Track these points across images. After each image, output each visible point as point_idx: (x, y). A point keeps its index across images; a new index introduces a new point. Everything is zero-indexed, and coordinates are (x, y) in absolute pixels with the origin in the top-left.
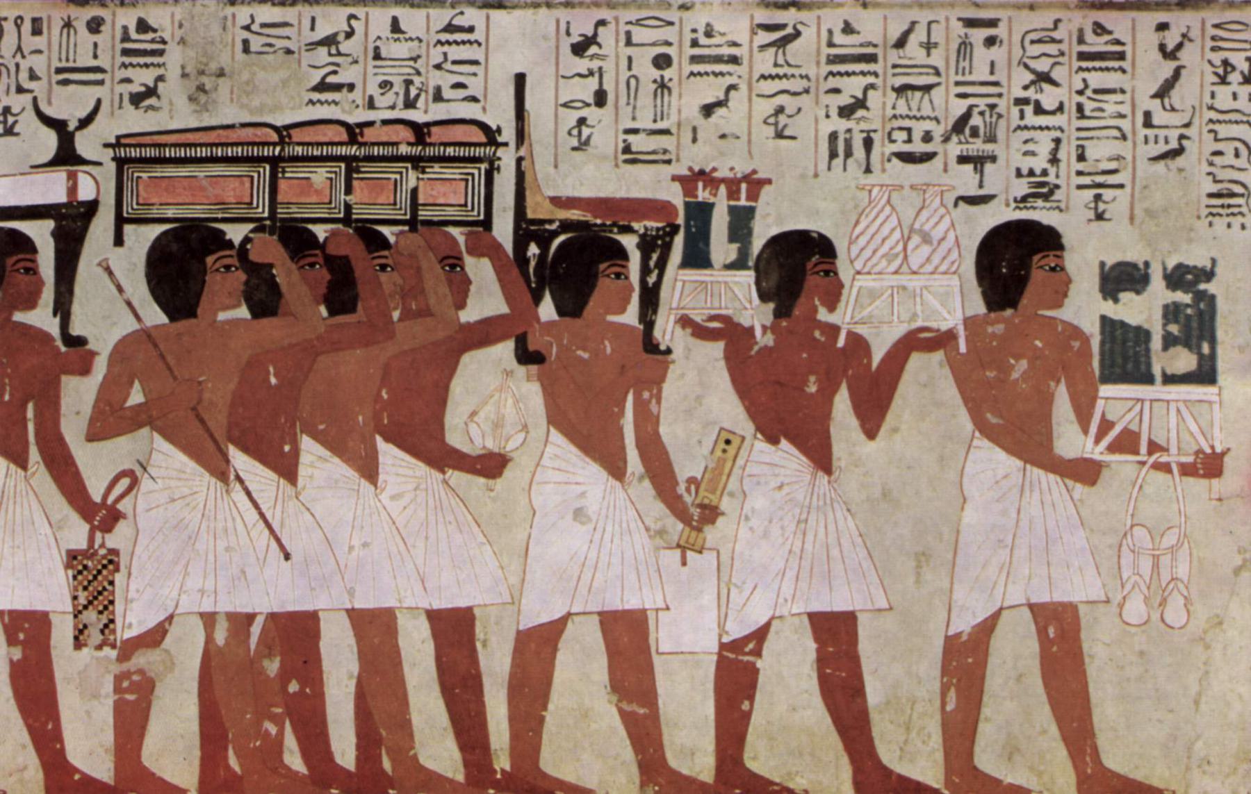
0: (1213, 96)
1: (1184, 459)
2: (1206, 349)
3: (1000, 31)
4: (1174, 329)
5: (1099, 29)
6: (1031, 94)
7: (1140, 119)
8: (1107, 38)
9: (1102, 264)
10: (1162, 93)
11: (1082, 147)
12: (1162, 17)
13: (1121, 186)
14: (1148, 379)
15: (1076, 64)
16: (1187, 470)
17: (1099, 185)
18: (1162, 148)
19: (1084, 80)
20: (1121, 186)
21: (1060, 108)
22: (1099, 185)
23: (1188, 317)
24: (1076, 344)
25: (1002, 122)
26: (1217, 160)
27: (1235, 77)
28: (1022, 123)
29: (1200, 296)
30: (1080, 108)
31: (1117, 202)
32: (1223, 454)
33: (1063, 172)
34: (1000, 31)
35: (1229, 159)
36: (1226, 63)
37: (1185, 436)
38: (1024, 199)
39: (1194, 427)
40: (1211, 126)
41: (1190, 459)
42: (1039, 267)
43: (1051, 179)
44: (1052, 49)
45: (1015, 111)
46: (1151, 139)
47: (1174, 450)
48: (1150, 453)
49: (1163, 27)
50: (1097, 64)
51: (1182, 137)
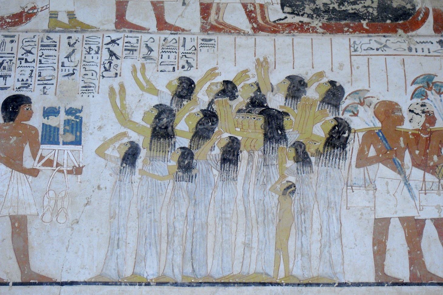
0: (85, 58)
1: (68, 169)
2: (78, 134)
3: (16, 39)
4: (68, 128)
5: (48, 38)
6: (24, 57)
7: (60, 64)
8: (51, 40)
9: (44, 108)
10: (67, 57)
11: (41, 72)
12: (70, 35)
13: (53, 84)
14: (57, 143)
15: (40, 48)
16: (69, 172)
17: (45, 83)
18: (67, 73)
19: (42, 53)
20: (53, 84)
21: (34, 61)
22: (45, 83)
23: (73, 124)
24: (33, 132)
25: (14, 65)
26: (86, 76)
27: (93, 52)
28: (21, 65)
29: (77, 117)
30: (40, 61)
31: (51, 89)
32: (83, 167)
33: (33, 80)
34: (16, 39)
35: (90, 76)
36: (90, 48)
37: (69, 161)
38: (19, 88)
39: (73, 159)
40: (84, 66)
41: (71, 169)
42: (23, 109)
43: (29, 82)
44: (32, 44)
45: (19, 62)
46: (64, 70)
47: (65, 166)
48: (57, 167)
49: (69, 38)
50: (47, 48)
51: (74, 70)
